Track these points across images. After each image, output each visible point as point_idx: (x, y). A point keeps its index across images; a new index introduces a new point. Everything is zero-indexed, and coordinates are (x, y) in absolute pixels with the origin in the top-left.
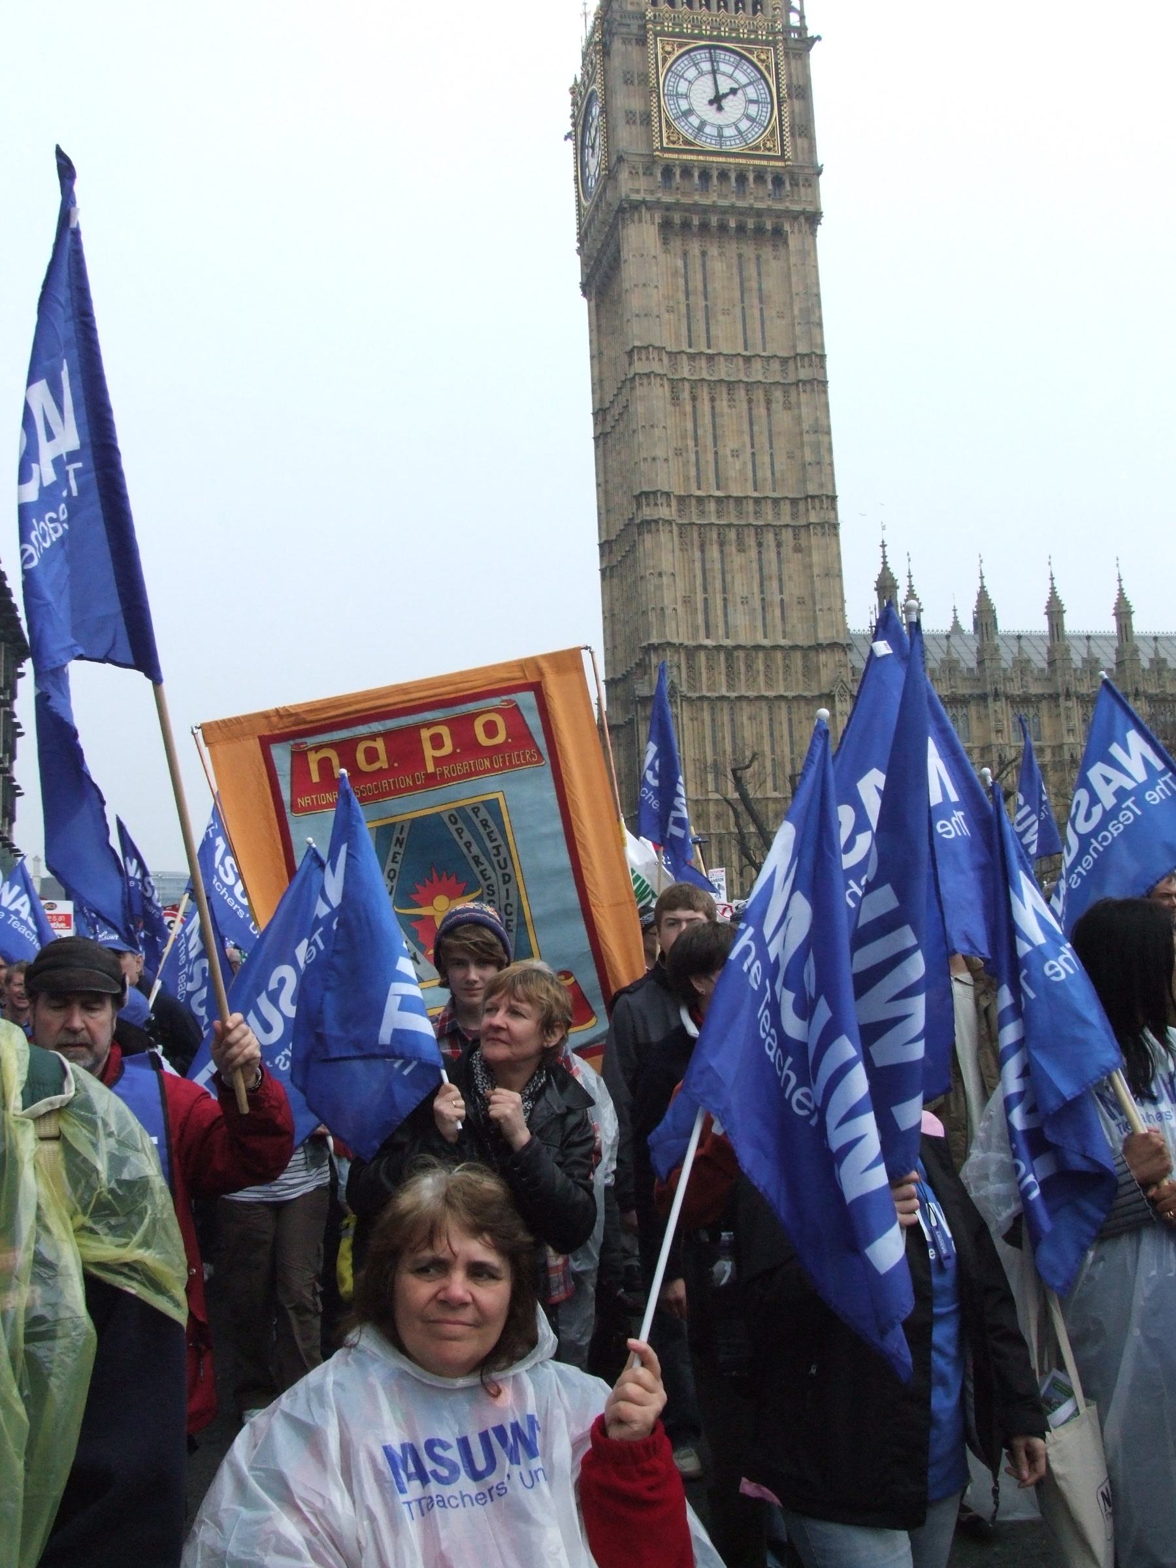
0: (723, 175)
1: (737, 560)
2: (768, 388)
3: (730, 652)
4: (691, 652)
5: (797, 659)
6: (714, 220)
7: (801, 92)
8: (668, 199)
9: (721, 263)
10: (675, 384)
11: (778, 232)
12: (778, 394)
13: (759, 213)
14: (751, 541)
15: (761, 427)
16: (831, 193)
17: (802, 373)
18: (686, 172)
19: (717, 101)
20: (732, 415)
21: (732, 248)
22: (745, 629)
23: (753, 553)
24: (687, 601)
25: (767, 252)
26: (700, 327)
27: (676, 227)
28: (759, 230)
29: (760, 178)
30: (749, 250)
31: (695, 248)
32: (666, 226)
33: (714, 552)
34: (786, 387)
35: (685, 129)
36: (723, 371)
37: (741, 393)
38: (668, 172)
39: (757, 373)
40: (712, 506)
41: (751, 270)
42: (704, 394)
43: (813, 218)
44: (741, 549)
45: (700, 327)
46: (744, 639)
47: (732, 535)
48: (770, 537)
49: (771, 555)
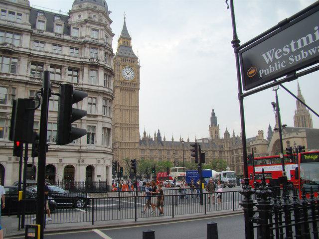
5: (133, 144)
7: (138, 73)
9: (127, 94)
15: (130, 115)
16: (142, 86)
17: (136, 109)
18: (124, 83)
19: (128, 74)
20: (127, 113)
21: (128, 92)
22: (127, 141)
25: (133, 93)
26: (124, 102)
27: (122, 89)
30: (131, 93)
32: (121, 89)
33: (124, 130)
42: (124, 112)
43: (139, 89)
44: (127, 130)
45: (124, 102)
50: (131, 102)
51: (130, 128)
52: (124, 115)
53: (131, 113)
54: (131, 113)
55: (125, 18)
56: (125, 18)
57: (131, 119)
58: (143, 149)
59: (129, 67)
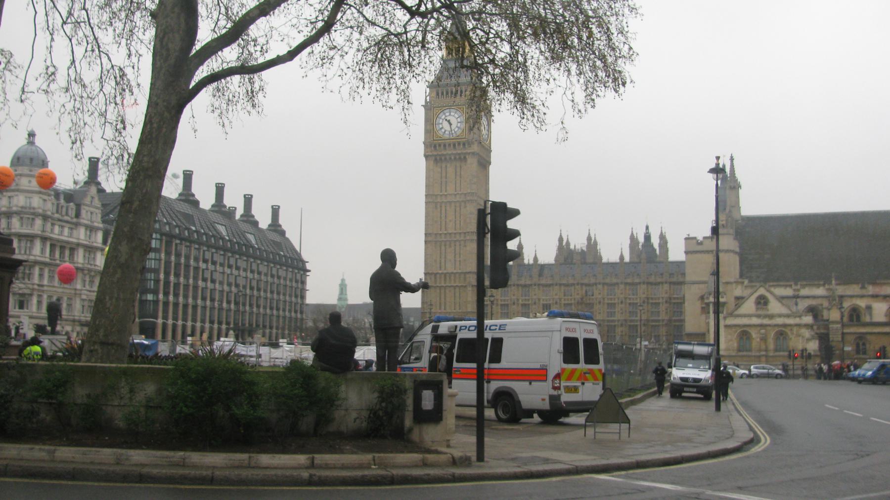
0: (450, 145)
3: (445, 274)
4: (435, 274)
5: (462, 276)
6: (448, 157)
8: (435, 153)
11: (465, 158)
12: (463, 204)
13: (459, 154)
14: (453, 245)
22: (450, 268)
23: (453, 248)
26: (443, 188)
28: (460, 158)
29: (459, 144)
30: (458, 164)
32: (436, 161)
33: (443, 248)
34: (465, 202)
35: (441, 133)
36: (449, 199)
37: (453, 204)
38: (435, 146)
39: (458, 198)
40: (443, 236)
41: (458, 170)
45: (443, 188)
46: (450, 271)
47: (448, 243)
48: (458, 243)
49: (457, 248)
50: (458, 185)
52: (443, 215)
53: (458, 209)
54: (458, 209)
57: (458, 222)
59: (450, 107)
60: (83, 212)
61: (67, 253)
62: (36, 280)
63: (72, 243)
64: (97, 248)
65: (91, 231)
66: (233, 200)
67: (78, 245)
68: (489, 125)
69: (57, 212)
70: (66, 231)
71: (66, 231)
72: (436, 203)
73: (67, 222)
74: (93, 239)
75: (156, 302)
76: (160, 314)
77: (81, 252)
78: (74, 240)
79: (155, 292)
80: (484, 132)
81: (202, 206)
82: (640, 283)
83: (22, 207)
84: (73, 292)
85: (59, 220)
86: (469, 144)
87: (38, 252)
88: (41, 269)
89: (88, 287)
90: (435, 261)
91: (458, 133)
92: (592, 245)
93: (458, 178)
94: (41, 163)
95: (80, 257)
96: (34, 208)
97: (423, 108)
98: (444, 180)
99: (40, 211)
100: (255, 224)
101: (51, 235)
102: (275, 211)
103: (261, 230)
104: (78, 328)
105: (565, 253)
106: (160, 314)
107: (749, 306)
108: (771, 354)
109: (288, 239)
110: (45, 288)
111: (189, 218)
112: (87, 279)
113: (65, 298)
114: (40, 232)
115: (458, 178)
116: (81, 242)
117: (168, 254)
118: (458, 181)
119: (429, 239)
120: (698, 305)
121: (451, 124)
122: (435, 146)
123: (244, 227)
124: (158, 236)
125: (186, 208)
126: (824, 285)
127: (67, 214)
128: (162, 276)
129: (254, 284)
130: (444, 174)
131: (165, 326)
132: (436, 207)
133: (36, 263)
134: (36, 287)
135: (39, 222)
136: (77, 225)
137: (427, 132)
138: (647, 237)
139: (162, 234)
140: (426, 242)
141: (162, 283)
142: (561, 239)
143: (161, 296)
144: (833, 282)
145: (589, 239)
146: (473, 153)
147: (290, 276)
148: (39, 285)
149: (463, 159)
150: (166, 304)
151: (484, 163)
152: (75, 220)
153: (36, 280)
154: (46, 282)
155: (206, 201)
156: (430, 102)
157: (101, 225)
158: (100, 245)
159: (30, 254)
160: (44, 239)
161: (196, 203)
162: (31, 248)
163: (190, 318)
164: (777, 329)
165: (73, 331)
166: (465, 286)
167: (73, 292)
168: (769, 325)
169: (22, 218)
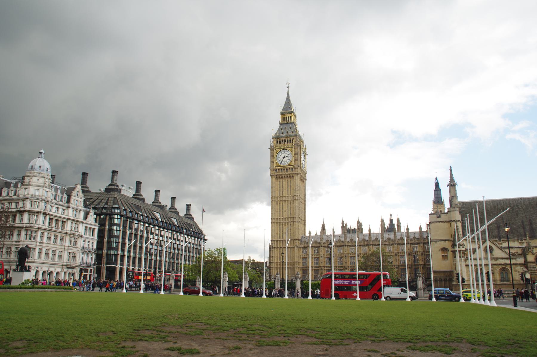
1: (284, 227)
2: (291, 201)
3: (282, 241)
9: (285, 182)
10: (277, 201)
11: (293, 176)
12: (292, 202)
18: (279, 170)
19: (284, 158)
21: (287, 179)
24: (277, 233)
25: (292, 179)
29: (289, 169)
30: (289, 180)
31: (281, 180)
33: (281, 226)
34: (293, 200)
36: (284, 199)
38: (276, 170)
41: (289, 183)
44: (285, 225)
48: (289, 224)
50: (289, 191)
51: (288, 222)
53: (289, 204)
54: (289, 204)
55: (288, 87)
56: (288, 87)
58: (304, 248)
59: (284, 149)
60: (72, 200)
61: (60, 224)
62: (38, 239)
63: (63, 218)
64: (80, 222)
65: (76, 211)
66: (165, 200)
67: (68, 219)
68: (305, 158)
69: (55, 199)
70: (60, 211)
71: (60, 211)
72: (277, 201)
73: (62, 206)
74: (77, 216)
75: (116, 255)
76: (119, 262)
77: (69, 223)
78: (66, 217)
79: (116, 249)
80: (303, 162)
81: (146, 202)
82: (393, 244)
83: (32, 195)
84: (63, 247)
85: (56, 204)
86: (295, 169)
87: (41, 222)
88: (42, 233)
89: (72, 245)
90: (277, 233)
91: (289, 163)
92: (360, 225)
93: (289, 187)
94: (46, 169)
95: (69, 226)
96: (39, 196)
97: (269, 150)
98: (281, 189)
99: (44, 198)
100: (177, 213)
101: (50, 213)
102: (188, 207)
103: (181, 217)
104: (65, 270)
105: (345, 229)
106: (119, 262)
107: (480, 253)
108: (498, 283)
109: (195, 222)
110: (44, 245)
111: (139, 208)
112: (73, 241)
113: (58, 252)
114: (42, 211)
115: (289, 187)
116: (69, 217)
117: (125, 227)
118: (289, 189)
119: (273, 221)
120: (440, 254)
121: (284, 158)
122: (276, 170)
123: (171, 214)
124: (119, 217)
125: (138, 203)
126: (518, 240)
127: (61, 201)
128: (120, 240)
129: (175, 246)
130: (281, 186)
131: (121, 270)
132: (277, 204)
133: (38, 228)
134: (38, 244)
135: (43, 204)
136: (68, 207)
137: (272, 162)
138: (391, 221)
139: (121, 216)
140: (272, 223)
141: (120, 244)
142: (343, 223)
143: (120, 252)
144: (528, 237)
145: (358, 222)
146: (298, 174)
147: (196, 242)
148: (40, 243)
149: (291, 177)
150: (123, 257)
151: (303, 180)
152: (66, 204)
153: (38, 239)
154: (45, 240)
155: (149, 199)
156: (273, 146)
157: (83, 208)
158: (82, 220)
159: (36, 224)
160: (45, 214)
161: (143, 200)
162: (37, 220)
163: (137, 265)
164: (500, 267)
165: (62, 271)
166: (294, 247)
167: (63, 247)
168: (496, 265)
169: (32, 201)
